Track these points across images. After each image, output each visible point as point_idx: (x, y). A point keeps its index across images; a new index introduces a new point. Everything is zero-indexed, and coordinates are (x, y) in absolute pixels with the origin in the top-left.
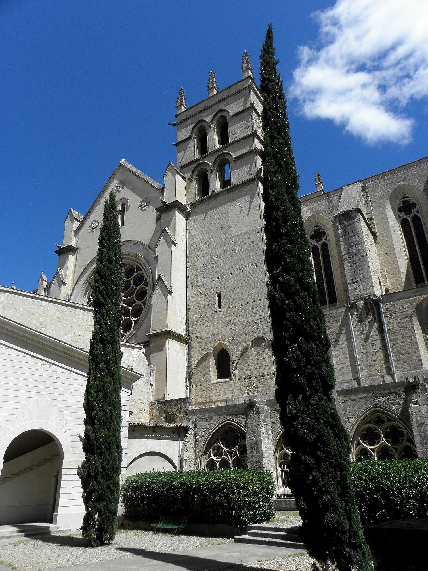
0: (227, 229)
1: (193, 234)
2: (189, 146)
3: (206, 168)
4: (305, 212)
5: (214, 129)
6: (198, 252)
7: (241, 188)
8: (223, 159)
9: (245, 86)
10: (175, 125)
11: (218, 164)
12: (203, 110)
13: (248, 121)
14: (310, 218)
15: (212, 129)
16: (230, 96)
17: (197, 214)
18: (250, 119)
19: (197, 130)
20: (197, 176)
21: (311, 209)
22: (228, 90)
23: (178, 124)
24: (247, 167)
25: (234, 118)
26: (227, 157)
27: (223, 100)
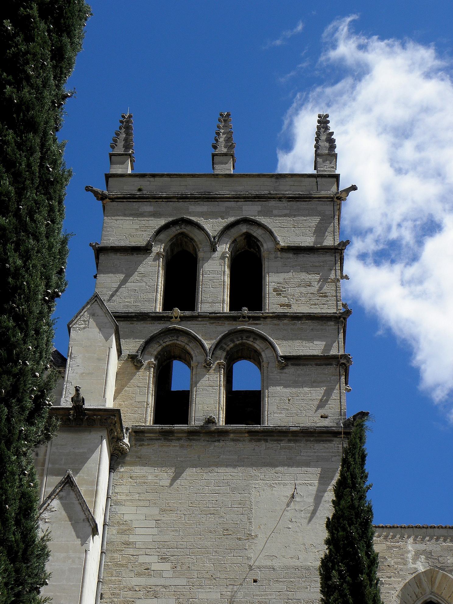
0: (240, 539)
1: (126, 518)
2: (141, 269)
3: (188, 348)
4: (410, 556)
5: (223, 257)
6: (139, 575)
7: (296, 441)
8: (242, 344)
9: (323, 193)
10: (102, 197)
11: (227, 354)
12: (195, 198)
13: (325, 280)
14: (422, 577)
15: (217, 255)
16: (280, 199)
17: (143, 461)
18: (332, 276)
19: (169, 238)
20: (156, 358)
21: (429, 555)
22: (273, 179)
23: (113, 200)
24: (318, 393)
25: (285, 255)
26: (255, 345)
27: (258, 198)
